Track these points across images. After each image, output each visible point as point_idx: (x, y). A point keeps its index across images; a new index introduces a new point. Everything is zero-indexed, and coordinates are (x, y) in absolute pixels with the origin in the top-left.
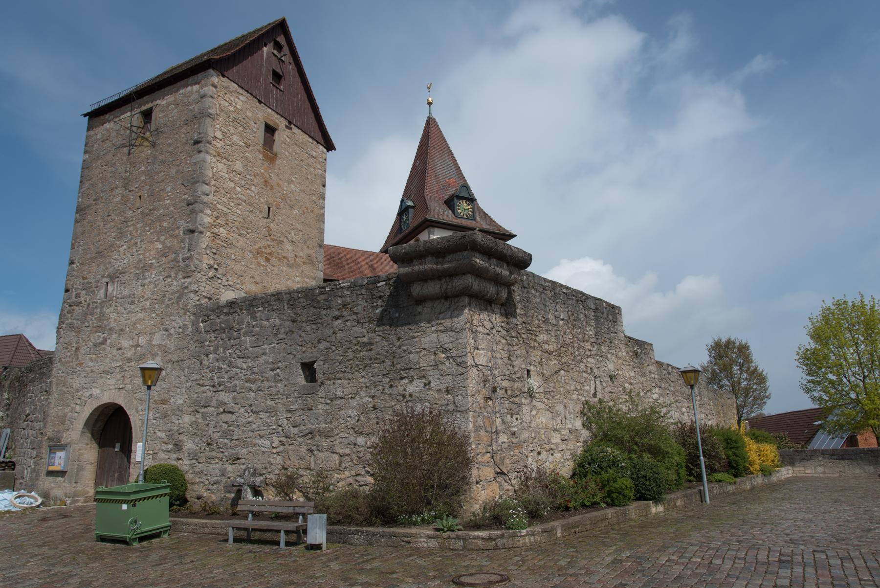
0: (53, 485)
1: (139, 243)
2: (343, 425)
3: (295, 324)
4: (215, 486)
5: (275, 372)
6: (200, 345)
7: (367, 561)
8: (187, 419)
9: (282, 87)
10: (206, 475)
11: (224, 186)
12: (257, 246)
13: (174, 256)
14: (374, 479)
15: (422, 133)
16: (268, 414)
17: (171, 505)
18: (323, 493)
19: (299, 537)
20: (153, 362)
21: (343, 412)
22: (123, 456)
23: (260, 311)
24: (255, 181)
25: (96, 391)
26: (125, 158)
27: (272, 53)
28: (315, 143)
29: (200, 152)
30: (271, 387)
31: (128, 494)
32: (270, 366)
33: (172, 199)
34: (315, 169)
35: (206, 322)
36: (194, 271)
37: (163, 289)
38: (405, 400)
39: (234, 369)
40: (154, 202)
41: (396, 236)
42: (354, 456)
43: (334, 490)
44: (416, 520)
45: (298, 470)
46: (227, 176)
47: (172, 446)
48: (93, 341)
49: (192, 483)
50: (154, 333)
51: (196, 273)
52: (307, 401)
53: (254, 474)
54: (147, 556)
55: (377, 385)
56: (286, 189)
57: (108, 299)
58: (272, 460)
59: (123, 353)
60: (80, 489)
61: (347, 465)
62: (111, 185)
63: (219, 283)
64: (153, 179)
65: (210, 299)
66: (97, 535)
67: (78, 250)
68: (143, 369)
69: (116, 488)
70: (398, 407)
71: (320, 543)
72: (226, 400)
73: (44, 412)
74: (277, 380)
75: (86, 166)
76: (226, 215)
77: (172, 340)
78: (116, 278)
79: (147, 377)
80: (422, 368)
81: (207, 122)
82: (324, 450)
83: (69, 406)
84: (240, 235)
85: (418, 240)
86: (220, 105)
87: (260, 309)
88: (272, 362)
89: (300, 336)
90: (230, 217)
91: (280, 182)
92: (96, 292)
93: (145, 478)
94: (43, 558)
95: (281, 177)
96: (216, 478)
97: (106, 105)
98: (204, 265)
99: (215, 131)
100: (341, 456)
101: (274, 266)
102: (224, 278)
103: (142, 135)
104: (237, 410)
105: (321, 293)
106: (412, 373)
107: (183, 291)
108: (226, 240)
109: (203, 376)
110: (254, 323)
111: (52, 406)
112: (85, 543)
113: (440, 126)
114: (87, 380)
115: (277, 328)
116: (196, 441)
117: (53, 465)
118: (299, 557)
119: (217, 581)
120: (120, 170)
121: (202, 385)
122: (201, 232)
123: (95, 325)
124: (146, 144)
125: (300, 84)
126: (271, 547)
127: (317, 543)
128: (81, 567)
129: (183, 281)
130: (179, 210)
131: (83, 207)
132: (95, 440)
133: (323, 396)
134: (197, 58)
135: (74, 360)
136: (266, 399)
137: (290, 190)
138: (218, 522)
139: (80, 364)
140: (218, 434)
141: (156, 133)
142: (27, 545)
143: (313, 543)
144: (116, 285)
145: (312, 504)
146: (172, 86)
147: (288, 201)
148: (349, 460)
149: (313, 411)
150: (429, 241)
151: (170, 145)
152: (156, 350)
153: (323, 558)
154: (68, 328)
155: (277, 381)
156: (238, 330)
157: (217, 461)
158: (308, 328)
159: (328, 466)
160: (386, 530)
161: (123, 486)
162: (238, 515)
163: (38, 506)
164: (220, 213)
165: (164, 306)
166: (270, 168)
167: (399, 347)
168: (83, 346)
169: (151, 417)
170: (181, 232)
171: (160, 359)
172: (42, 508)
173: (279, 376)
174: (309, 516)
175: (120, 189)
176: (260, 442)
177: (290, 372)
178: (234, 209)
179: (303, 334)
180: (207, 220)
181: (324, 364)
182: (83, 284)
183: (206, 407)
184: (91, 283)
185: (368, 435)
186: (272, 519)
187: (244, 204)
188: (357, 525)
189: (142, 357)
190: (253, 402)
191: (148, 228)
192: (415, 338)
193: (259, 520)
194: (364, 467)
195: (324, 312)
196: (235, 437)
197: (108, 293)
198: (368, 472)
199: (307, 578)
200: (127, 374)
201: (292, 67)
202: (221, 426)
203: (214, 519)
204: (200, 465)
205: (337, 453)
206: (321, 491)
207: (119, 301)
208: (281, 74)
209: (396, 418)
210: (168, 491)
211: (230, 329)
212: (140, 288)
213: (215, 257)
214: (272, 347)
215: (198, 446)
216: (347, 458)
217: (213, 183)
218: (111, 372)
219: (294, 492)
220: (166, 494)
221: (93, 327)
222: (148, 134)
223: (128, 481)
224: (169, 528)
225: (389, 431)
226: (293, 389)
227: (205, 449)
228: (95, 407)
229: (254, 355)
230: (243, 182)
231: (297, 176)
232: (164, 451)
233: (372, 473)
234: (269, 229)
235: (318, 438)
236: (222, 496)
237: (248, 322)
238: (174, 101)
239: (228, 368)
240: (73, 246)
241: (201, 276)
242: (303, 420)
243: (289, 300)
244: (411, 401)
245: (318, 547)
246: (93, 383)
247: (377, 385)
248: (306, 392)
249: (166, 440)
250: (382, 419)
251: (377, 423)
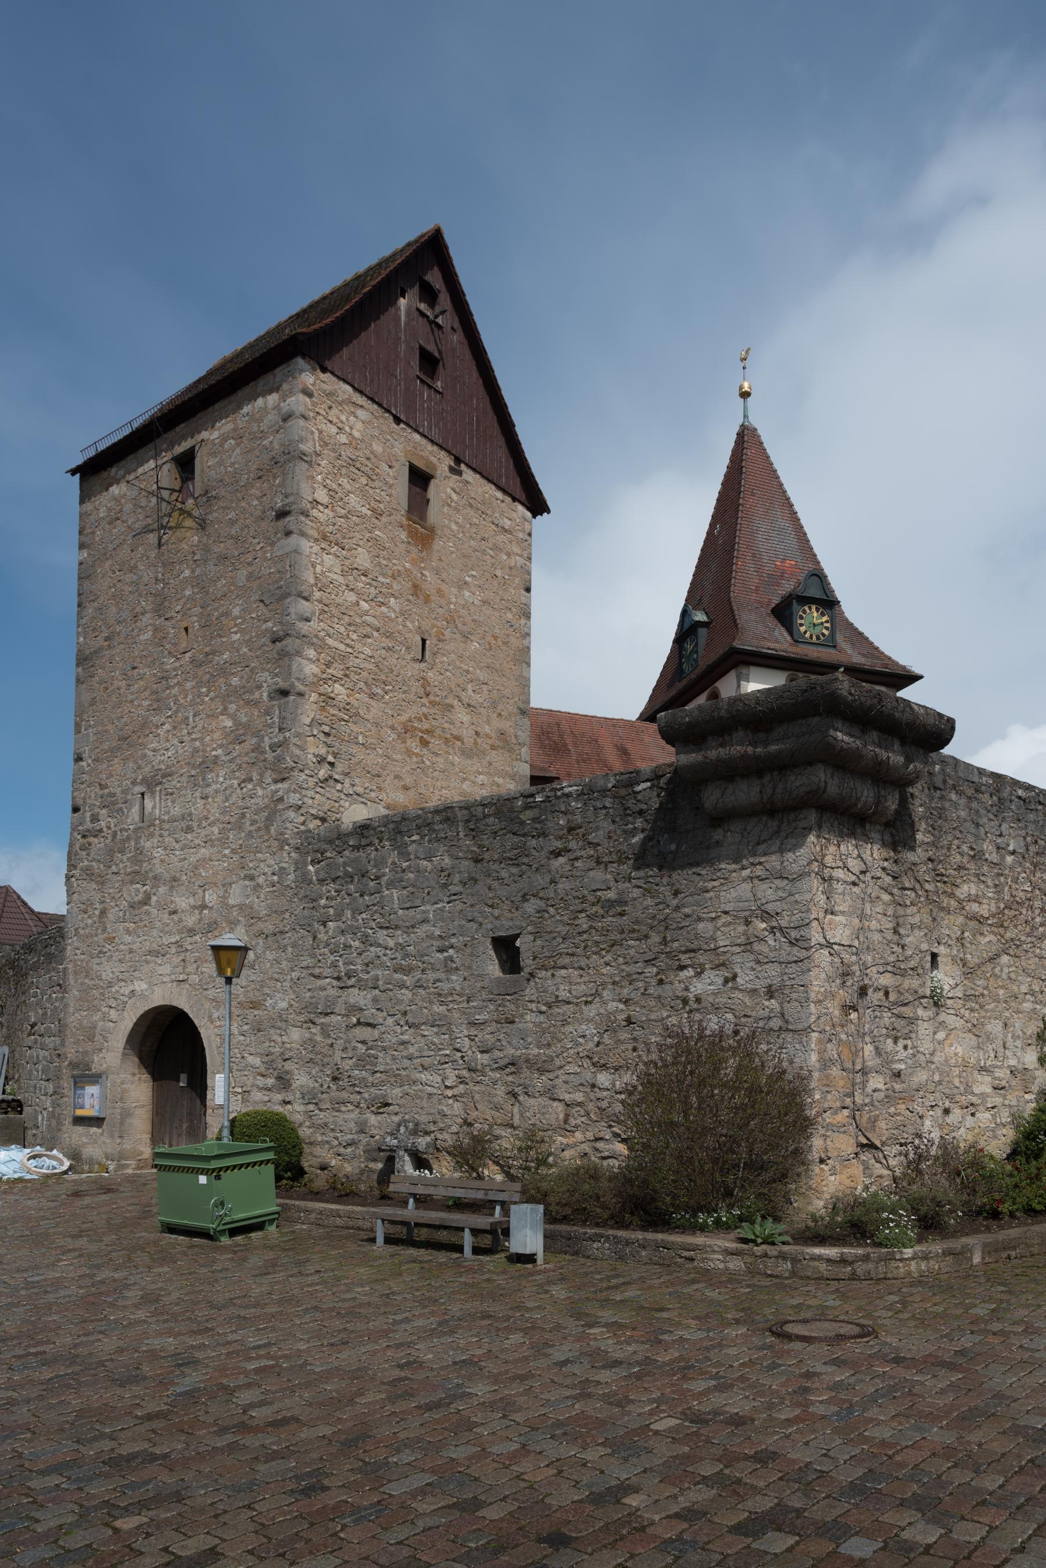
0: (84, 1139)
1: (191, 719)
2: (572, 1051)
3: (479, 866)
4: (349, 1150)
5: (445, 954)
6: (311, 905)
7: (616, 1287)
9: (439, 384)
10: (333, 1130)
11: (338, 600)
12: (404, 718)
13: (254, 741)
14: (629, 1148)
15: (727, 461)
16: (435, 1029)
17: (278, 1178)
18: (537, 1169)
19: (496, 1241)
20: (231, 936)
21: (570, 1028)
22: (194, 1095)
23: (414, 841)
24: (396, 586)
25: (140, 986)
26: (153, 554)
27: (418, 309)
28: (508, 500)
29: (288, 533)
30: (439, 980)
31: (207, 1159)
32: (436, 943)
33: (242, 631)
35: (319, 863)
36: (292, 769)
37: (240, 803)
38: (687, 1008)
39: (372, 949)
41: (670, 685)
42: (591, 1106)
43: (555, 1164)
44: (705, 1221)
45: (491, 1126)
48: (128, 898)
49: (311, 1143)
50: (230, 884)
51: (296, 773)
52: (504, 1006)
53: (415, 1132)
54: (245, 1259)
55: (633, 980)
56: (454, 600)
57: (147, 823)
58: (445, 1109)
60: (129, 1147)
61: (578, 1122)
62: (134, 609)
63: (338, 791)
64: (208, 593)
65: (323, 820)
66: (162, 1222)
67: (88, 735)
68: (216, 949)
69: (184, 1147)
70: (674, 1020)
71: (533, 1252)
72: (362, 1003)
73: (60, 1020)
74: (450, 970)
75: (85, 574)
76: (344, 657)
77: (262, 896)
78: (157, 785)
79: (224, 962)
80: (721, 950)
81: (297, 472)
82: (537, 1094)
83: (99, 1010)
84: (372, 696)
85: (715, 696)
87: (414, 838)
89: (490, 888)
90: (352, 662)
91: (443, 587)
92: (126, 811)
93: (232, 1133)
94: (80, 1256)
95: (444, 575)
96: (350, 1137)
97: (108, 448)
98: (310, 756)
99: (314, 489)
100: (568, 1105)
101: (437, 755)
102: (347, 780)
103: (179, 505)
104: (381, 1020)
105: (527, 807)
106: (701, 958)
107: (275, 806)
108: (346, 708)
109: (319, 961)
111: (71, 1010)
112: (143, 1234)
113: (766, 445)
114: (124, 967)
115: (446, 873)
116: (314, 1072)
117: (82, 1107)
118: (498, 1274)
119: (360, 1306)
120: (146, 579)
122: (301, 695)
124: (189, 523)
125: (475, 374)
126: (449, 1254)
127: (528, 1251)
128: (141, 1273)
129: (273, 788)
131: (87, 652)
132: (146, 1068)
133: (534, 998)
134: (269, 334)
135: (99, 931)
136: (431, 1002)
137: (462, 602)
138: (359, 1208)
139: (109, 939)
140: (351, 1062)
141: (205, 499)
142: (55, 1234)
143: (521, 1251)
144: (157, 798)
145: (517, 1186)
146: (225, 402)
147: (459, 625)
148: (582, 1113)
149: (515, 1026)
150: (741, 699)
151: (232, 522)
152: (235, 914)
153: (538, 1277)
154: (85, 877)
155: (449, 971)
156: (377, 878)
157: (350, 1107)
158: (504, 874)
159: (544, 1121)
160: (650, 1236)
161: (197, 1145)
162: (390, 1198)
163: (65, 1172)
164: (333, 654)
165: (243, 835)
166: (422, 560)
167: (677, 908)
168: (113, 907)
169: (235, 1031)
170: (265, 694)
171: (243, 931)
172: (71, 1176)
173: (452, 961)
174: (513, 1207)
175: (148, 615)
176: (423, 1077)
177: (472, 955)
178: (358, 646)
179: (496, 884)
180: (310, 669)
181: (534, 940)
182: (102, 797)
184: (114, 795)
185: (616, 1070)
186: (449, 1208)
187: (376, 634)
188: (597, 1225)
189: (212, 927)
190: (408, 1008)
191: (204, 690)
192: (707, 891)
193: (426, 1209)
194: (610, 1126)
195: (534, 842)
196: (381, 1068)
197: (146, 813)
198: (616, 1135)
199: (511, 1309)
200: (189, 957)
201: (456, 338)
202: (354, 1049)
203: (349, 1204)
204: (322, 1115)
205: (560, 1100)
206: (533, 1165)
207: (166, 826)
208: (436, 354)
209: (669, 1040)
210: (271, 1155)
211: (363, 876)
212: (200, 803)
213: (329, 740)
214: (439, 909)
216: (579, 1108)
218: (162, 952)
219: (485, 1165)
220: (268, 1161)
221: (127, 874)
222: (190, 502)
223: (205, 1137)
224: (276, 1216)
225: (656, 1064)
226: (478, 985)
228: (142, 1012)
229: (407, 924)
230: (372, 590)
231: (474, 573)
232: (260, 1089)
233: (624, 1136)
234: (425, 682)
235: (526, 1072)
236: (363, 1165)
237: (394, 863)
238: (235, 430)
239: (362, 946)
240: (77, 726)
241: (304, 777)
242: (499, 1040)
243: (468, 821)
244: (697, 1010)
245: (530, 1259)
247: (633, 980)
248: (502, 990)
249: (262, 1070)
250: (644, 1042)
251: (635, 1049)
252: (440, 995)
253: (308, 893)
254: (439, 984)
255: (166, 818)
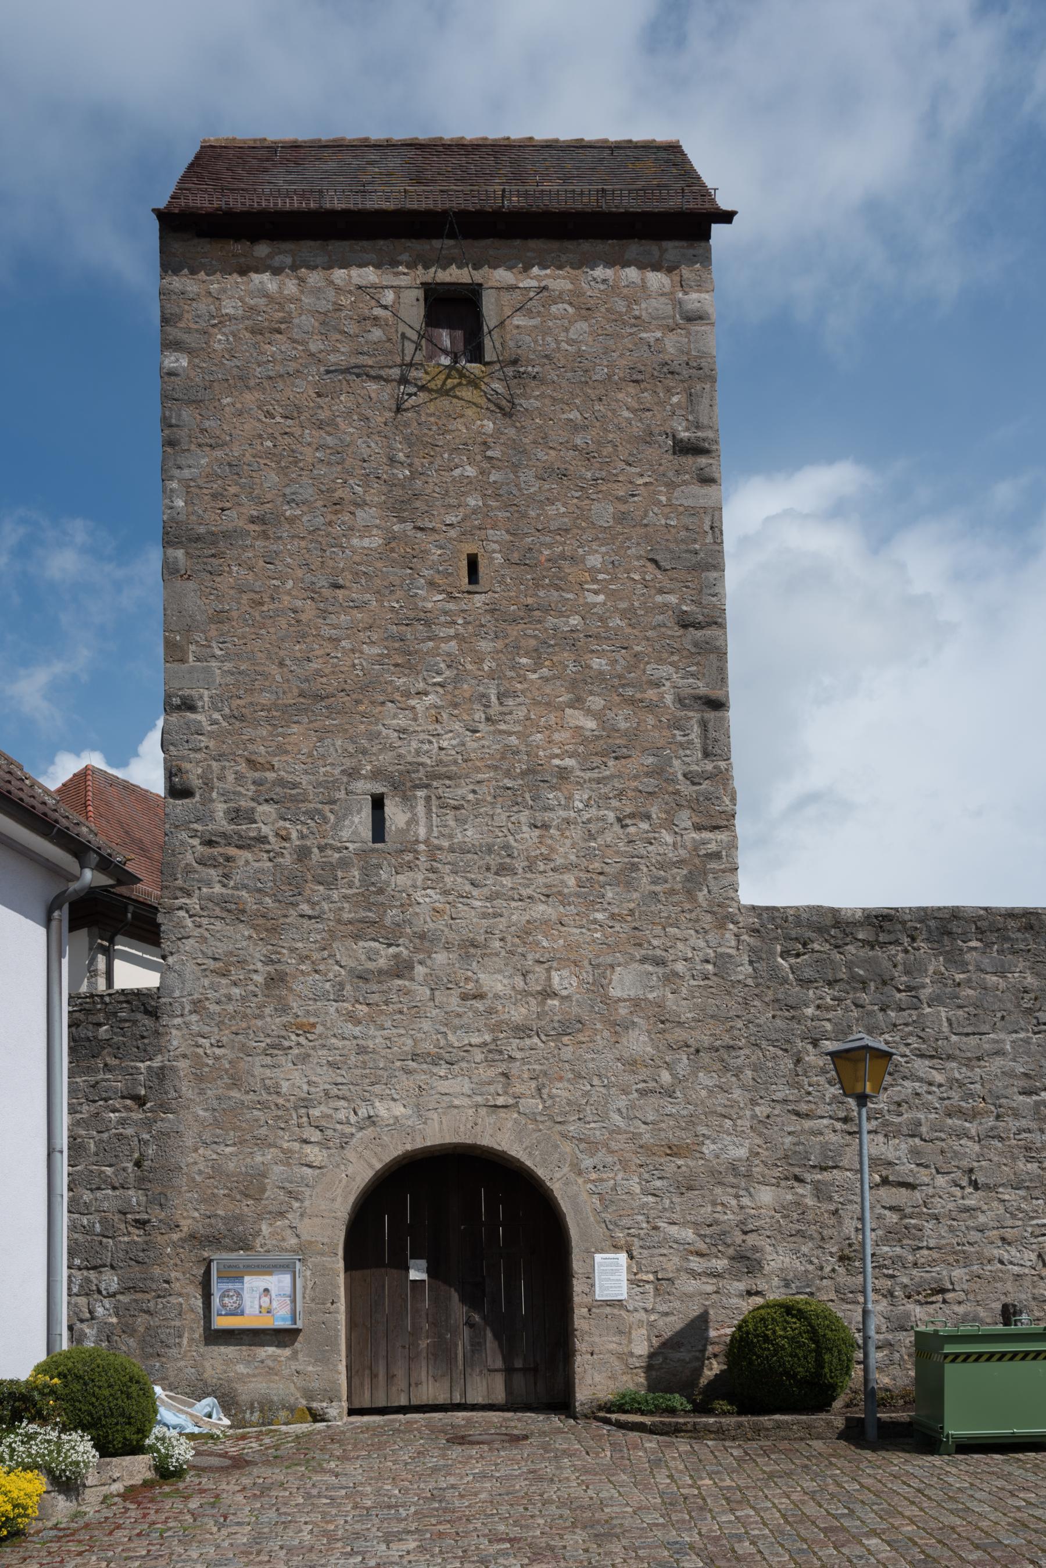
5: (1035, 1098)
8: (766, 1196)
16: (1022, 1193)
32: (1023, 1083)
39: (906, 1083)
40: (537, 586)
47: (726, 1262)
59: (490, 1011)
72: (891, 1156)
87: (974, 944)
88: (1025, 1075)
104: (926, 1180)
109: (809, 1093)
110: (959, 977)
115: (1032, 995)
121: (807, 1116)
123: (346, 916)
130: (650, 633)
171: (644, 1038)
183: (824, 1169)
211: (884, 983)
212: (530, 835)
214: (1021, 1040)
215: (811, 1262)
227: (833, 1270)
229: (969, 1055)
246: (373, 1084)
252: (1028, 1149)
253: (781, 996)
254: (1024, 1135)
255: (446, 844)
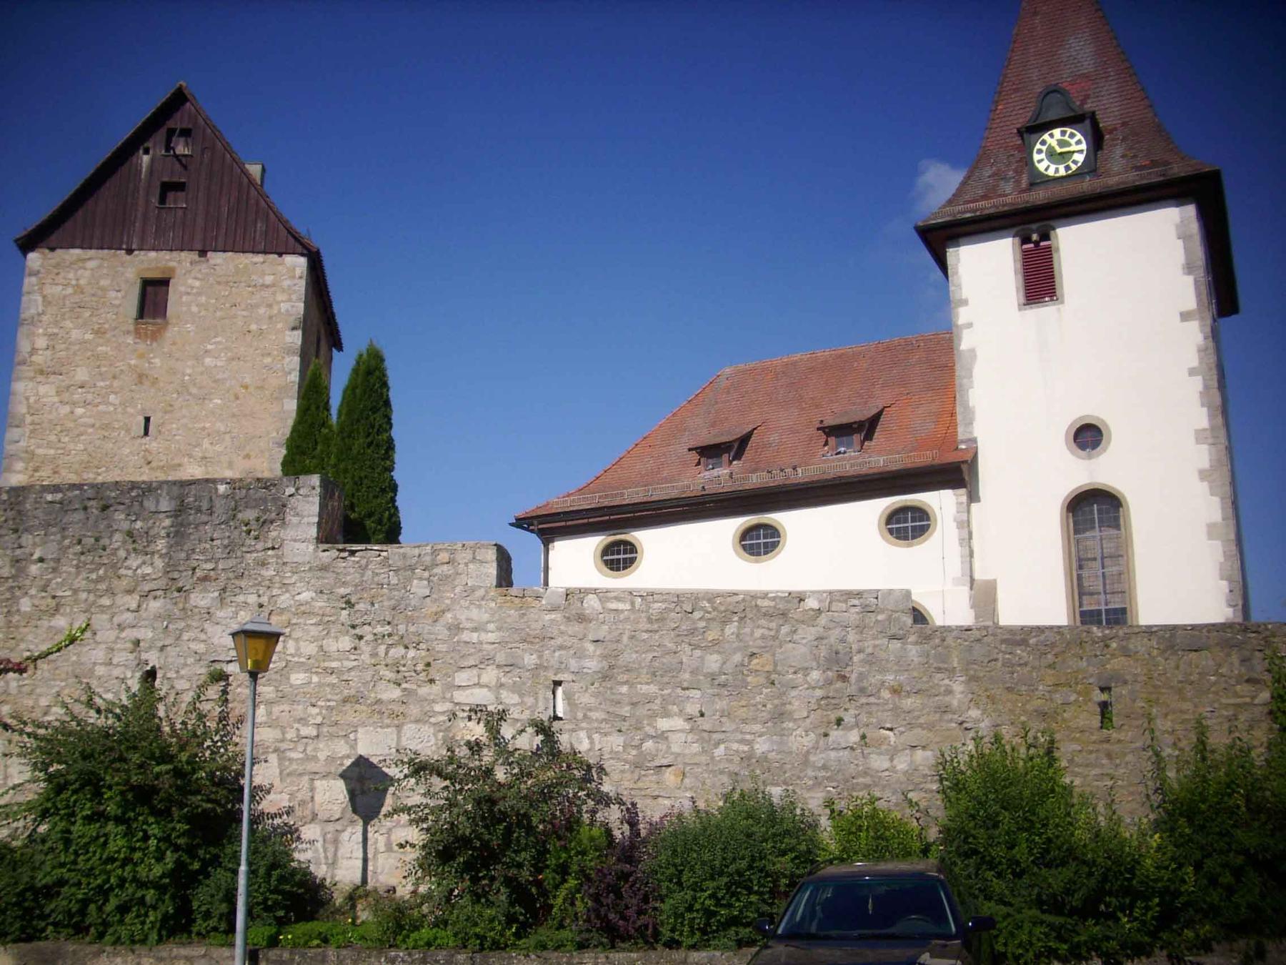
34: (270, 306)
46: (56, 399)
86: (44, 297)
166: (152, 351)
217: (29, 419)
